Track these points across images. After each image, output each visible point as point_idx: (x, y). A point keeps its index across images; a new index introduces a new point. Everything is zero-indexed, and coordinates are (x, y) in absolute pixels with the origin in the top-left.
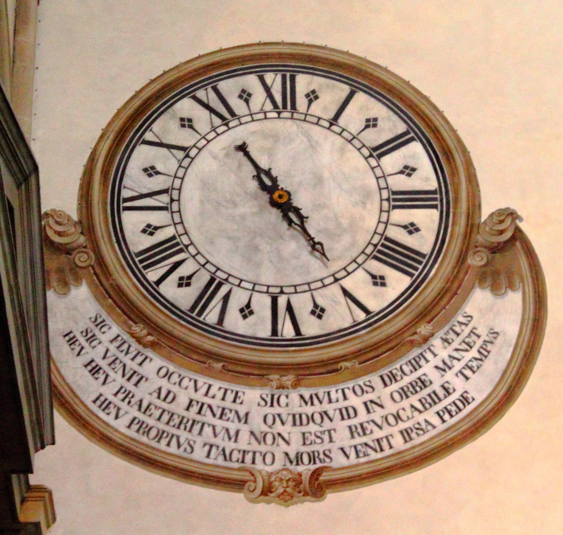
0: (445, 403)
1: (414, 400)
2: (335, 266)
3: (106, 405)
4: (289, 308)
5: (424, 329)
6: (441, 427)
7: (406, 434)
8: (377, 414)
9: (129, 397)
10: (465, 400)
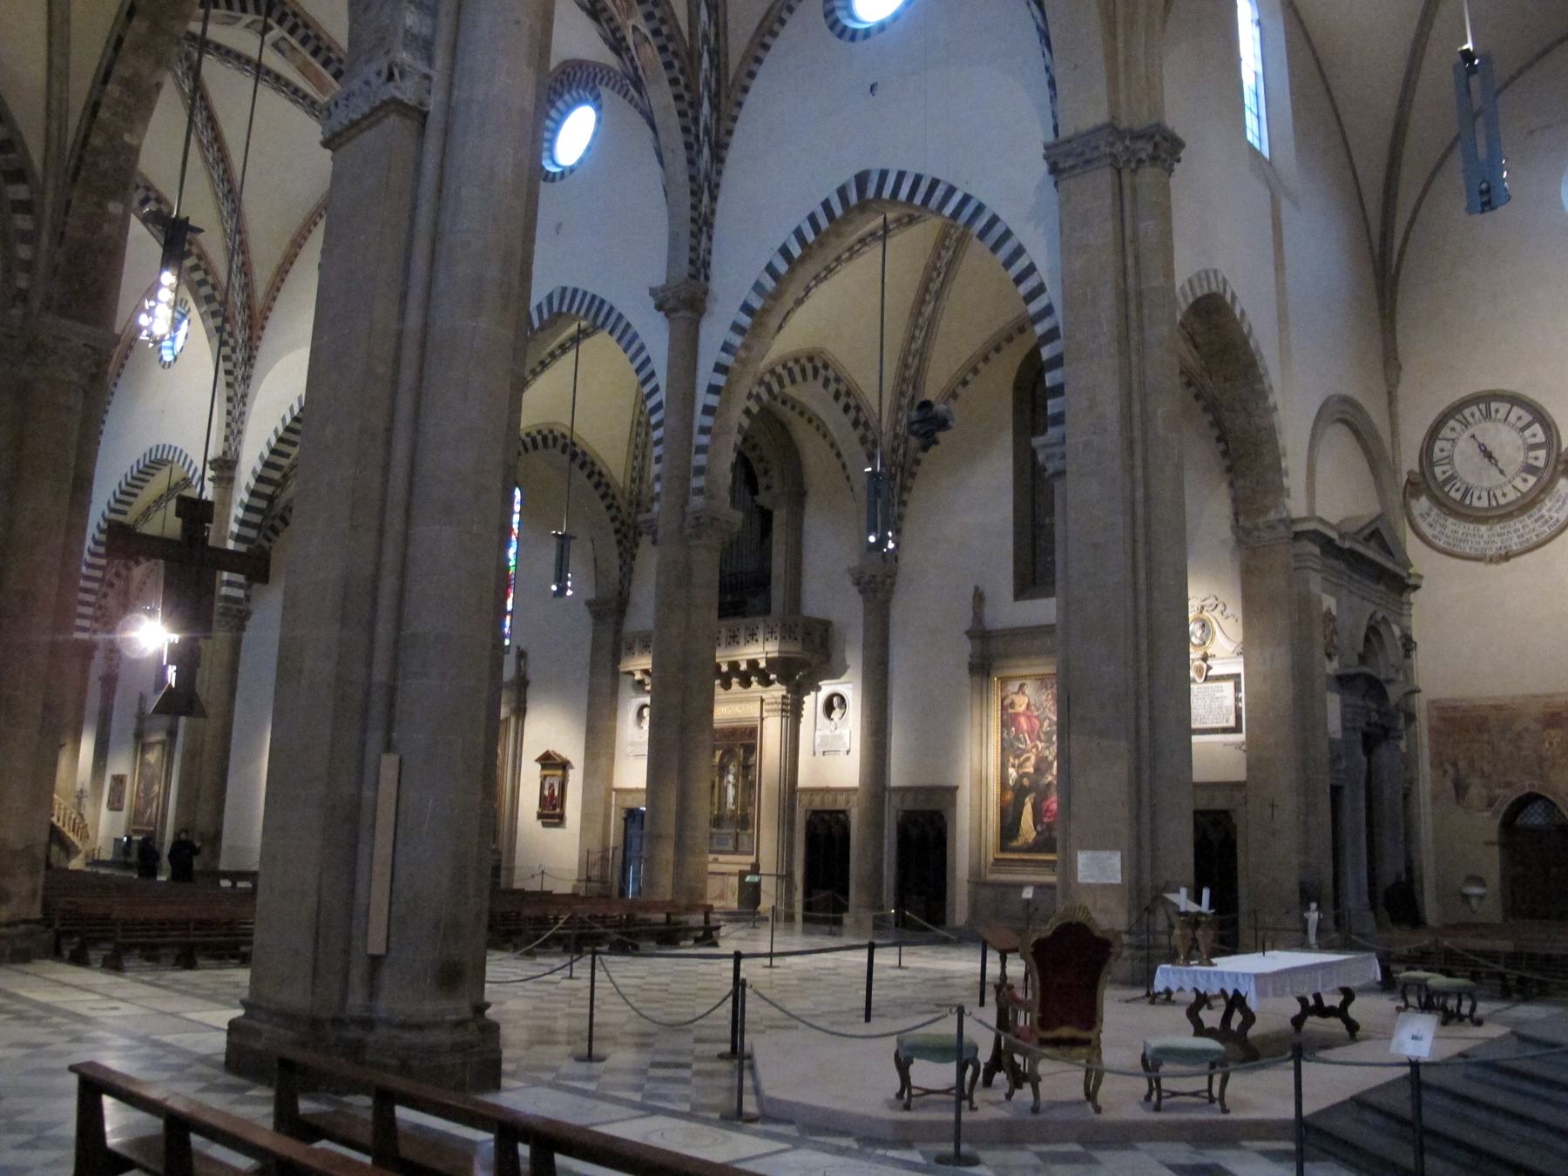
0: (1551, 522)
1: (1540, 523)
2: (1509, 477)
3: (1436, 537)
4: (1495, 496)
5: (1542, 496)
6: (1549, 532)
7: (1537, 536)
8: (1527, 530)
9: (1442, 534)
10: (1557, 521)
